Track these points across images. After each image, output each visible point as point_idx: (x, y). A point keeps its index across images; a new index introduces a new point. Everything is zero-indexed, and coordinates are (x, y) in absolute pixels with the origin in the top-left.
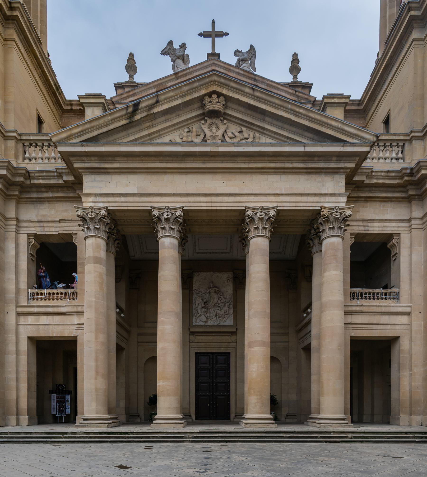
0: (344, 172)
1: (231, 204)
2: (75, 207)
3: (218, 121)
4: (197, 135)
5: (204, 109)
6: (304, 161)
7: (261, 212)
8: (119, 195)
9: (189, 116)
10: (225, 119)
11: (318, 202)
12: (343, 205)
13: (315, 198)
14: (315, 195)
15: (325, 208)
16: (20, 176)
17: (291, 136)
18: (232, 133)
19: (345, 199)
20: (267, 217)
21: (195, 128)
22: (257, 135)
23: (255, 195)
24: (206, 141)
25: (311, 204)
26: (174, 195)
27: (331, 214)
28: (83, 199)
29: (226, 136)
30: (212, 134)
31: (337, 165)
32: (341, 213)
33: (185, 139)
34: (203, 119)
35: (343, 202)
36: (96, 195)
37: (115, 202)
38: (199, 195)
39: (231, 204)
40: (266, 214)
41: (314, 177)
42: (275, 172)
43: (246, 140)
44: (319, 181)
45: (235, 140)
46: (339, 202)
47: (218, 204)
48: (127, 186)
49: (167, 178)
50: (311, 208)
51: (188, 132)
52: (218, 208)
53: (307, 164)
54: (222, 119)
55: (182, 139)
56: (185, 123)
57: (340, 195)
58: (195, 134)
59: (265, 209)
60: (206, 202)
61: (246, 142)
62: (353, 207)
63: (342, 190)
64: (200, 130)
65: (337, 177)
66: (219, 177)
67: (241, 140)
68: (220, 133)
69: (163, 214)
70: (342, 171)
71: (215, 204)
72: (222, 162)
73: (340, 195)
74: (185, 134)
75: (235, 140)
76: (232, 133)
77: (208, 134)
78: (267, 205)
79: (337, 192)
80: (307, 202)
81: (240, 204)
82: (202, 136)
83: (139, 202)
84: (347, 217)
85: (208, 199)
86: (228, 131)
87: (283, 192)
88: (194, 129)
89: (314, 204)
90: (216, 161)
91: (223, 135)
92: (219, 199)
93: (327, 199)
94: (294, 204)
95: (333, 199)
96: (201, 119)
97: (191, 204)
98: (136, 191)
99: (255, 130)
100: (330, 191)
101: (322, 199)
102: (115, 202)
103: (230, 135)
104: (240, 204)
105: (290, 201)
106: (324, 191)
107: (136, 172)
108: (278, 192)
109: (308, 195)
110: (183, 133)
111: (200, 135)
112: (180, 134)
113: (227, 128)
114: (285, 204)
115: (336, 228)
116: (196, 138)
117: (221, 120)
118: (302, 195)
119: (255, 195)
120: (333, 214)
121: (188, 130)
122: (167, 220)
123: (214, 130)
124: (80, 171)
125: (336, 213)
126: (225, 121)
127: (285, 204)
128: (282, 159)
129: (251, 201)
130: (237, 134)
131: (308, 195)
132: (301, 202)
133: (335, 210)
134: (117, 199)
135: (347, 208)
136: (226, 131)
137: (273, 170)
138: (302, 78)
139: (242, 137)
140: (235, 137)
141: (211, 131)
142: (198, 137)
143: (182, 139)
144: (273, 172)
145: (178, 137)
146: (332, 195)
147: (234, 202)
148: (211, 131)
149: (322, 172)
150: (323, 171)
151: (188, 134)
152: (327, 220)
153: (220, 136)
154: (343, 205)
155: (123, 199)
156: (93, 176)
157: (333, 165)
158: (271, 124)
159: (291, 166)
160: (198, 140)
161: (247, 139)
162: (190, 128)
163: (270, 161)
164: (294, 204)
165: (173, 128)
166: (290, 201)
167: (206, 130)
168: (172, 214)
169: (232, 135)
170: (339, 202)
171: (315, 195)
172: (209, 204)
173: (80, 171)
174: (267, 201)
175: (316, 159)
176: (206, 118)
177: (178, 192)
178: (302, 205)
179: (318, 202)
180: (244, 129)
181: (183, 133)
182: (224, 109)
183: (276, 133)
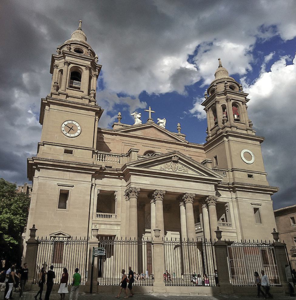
1: (180, 191)
11: (207, 193)
19: (215, 193)
39: (180, 191)
47: (176, 190)
68: (176, 167)
77: (173, 166)
79: (212, 191)
92: (177, 188)
93: (210, 192)
95: (211, 192)
98: (149, 183)
101: (208, 192)
153: (176, 168)
155: (145, 185)
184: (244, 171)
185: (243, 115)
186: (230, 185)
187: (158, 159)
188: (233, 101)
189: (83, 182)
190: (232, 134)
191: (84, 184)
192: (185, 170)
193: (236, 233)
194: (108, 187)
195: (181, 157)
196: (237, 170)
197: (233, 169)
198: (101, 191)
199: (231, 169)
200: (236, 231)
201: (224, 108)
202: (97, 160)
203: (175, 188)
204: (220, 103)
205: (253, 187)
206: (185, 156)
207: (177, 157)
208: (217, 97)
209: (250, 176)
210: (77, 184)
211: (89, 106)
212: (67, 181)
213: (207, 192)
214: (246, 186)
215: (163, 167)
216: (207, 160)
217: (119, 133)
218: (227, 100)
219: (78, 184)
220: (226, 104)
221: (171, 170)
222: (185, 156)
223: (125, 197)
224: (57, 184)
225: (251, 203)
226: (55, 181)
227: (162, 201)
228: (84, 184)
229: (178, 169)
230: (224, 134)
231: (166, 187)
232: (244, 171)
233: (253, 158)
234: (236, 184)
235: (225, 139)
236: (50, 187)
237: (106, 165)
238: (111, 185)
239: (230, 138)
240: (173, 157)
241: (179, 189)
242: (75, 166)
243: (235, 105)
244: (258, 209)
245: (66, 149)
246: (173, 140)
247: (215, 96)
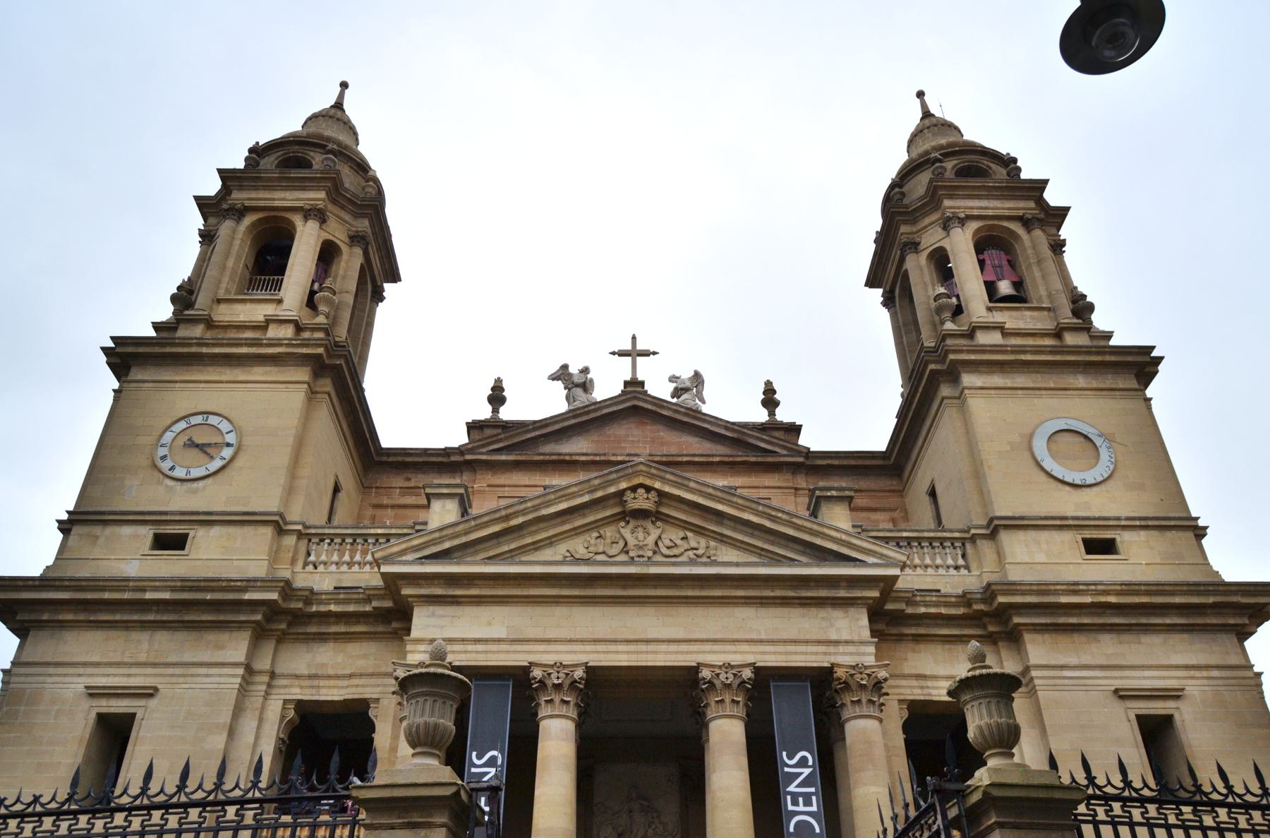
0: (865, 604)
2: (393, 663)
3: (649, 525)
4: (613, 543)
5: (624, 506)
7: (726, 673)
9: (599, 516)
10: (658, 519)
11: (825, 654)
12: (870, 660)
13: (820, 647)
14: (819, 642)
15: (839, 665)
17: (766, 546)
18: (671, 540)
19: (872, 649)
20: (737, 682)
21: (609, 532)
22: (712, 544)
23: (715, 641)
24: (627, 552)
25: (813, 658)
26: (571, 641)
27: (852, 675)
28: (409, 647)
29: (660, 544)
30: (638, 543)
31: (849, 593)
32: (869, 675)
33: (591, 549)
34: (623, 519)
35: (869, 654)
37: (466, 652)
38: (616, 641)
40: (735, 675)
41: (814, 611)
42: (746, 603)
43: (695, 551)
44: (823, 618)
45: (675, 551)
46: (864, 654)
47: (650, 657)
48: (489, 624)
49: (560, 611)
50: (815, 665)
51: (597, 538)
52: (649, 664)
53: (799, 591)
54: (654, 519)
55: (587, 548)
56: (594, 526)
57: (862, 643)
58: (608, 541)
59: (732, 667)
60: (628, 652)
61: (695, 555)
62: (888, 664)
63: (866, 633)
64: (618, 536)
65: (852, 611)
66: (650, 610)
67: (685, 551)
68: (651, 540)
69: (549, 674)
70: (859, 602)
71: (644, 657)
72: (655, 587)
73: (862, 643)
74: (593, 542)
75: (675, 551)
76: (671, 540)
77: (632, 542)
78: (736, 659)
79: (856, 638)
80: (806, 653)
81: (689, 657)
82: (621, 544)
83: (508, 652)
84: (879, 682)
85: (632, 647)
86: (663, 536)
87: (763, 637)
88: (608, 534)
89: (819, 658)
90: (646, 586)
91: (656, 543)
92: (651, 647)
93: (841, 649)
94: (783, 658)
95: (851, 649)
96: (620, 520)
97: (602, 657)
98: (503, 636)
99: (708, 536)
100: (845, 636)
101: (832, 649)
102: (466, 652)
103: (668, 543)
104: (689, 657)
105: (775, 653)
106: (834, 637)
107: (508, 602)
108: (754, 636)
109: (807, 642)
110: (589, 539)
111: (617, 543)
112: (585, 540)
113: (662, 533)
114: (768, 657)
115: (864, 701)
116: (612, 547)
117: (652, 522)
118: (795, 642)
119: (715, 641)
120: (856, 676)
121: (597, 535)
122: (558, 687)
123: (641, 535)
124: (410, 599)
125: (859, 675)
126: (659, 524)
127: (768, 657)
128: (757, 583)
129: (709, 652)
130: (679, 542)
131: (807, 642)
132: (796, 653)
133: (857, 669)
134: (470, 647)
135: (878, 666)
136: (660, 537)
137: (743, 601)
138: (783, 415)
139: (687, 546)
140: (676, 545)
141: (637, 538)
142: (615, 545)
143: (587, 548)
144: (743, 603)
145: (581, 546)
146: (847, 642)
147: (677, 652)
148: (637, 538)
149: (826, 604)
150: (826, 601)
151: (599, 540)
152: (847, 686)
154: (870, 660)
155: (480, 647)
156: (431, 608)
157: (842, 593)
158: (734, 529)
159: (772, 594)
160: (615, 550)
161: (697, 549)
162: (602, 532)
163: (737, 587)
164: (783, 658)
165: (573, 533)
166: (775, 653)
167: (628, 535)
168: (567, 674)
169: (670, 544)
170: (864, 654)
171: (819, 642)
172: (634, 657)
173: (410, 599)
174: (735, 652)
175: (812, 584)
176: (627, 519)
177: (578, 636)
178: (798, 659)
179: (825, 654)
180: (689, 534)
181: (589, 539)
182: (657, 507)
183: (742, 542)
184: (1059, 524)
185: (1037, 274)
186: (976, 607)
187: (545, 512)
188: (974, 225)
189: (203, 671)
190: (973, 357)
191: (207, 676)
192: (700, 552)
194: (332, 682)
195: (667, 489)
196: (1019, 524)
197: (991, 520)
199: (987, 527)
202: (306, 564)
203: (643, 647)
204: (922, 247)
205: (1112, 599)
206: (686, 482)
208: (904, 229)
209: (1100, 547)
210: (174, 680)
211: (281, 345)
212: (134, 671)
213: (822, 649)
214: (1064, 599)
215: (581, 552)
216: (821, 489)
217: (484, 457)
219: (181, 680)
221: (623, 558)
222: (679, 480)
224: (87, 687)
225: (1116, 691)
226: (80, 675)
227: (573, 719)
228: (207, 676)
229: (665, 551)
230: (932, 366)
231: (589, 648)
232: (1059, 524)
233: (1104, 454)
236: (56, 708)
237: (340, 580)
238: (348, 672)
239: (968, 379)
240: (629, 496)
241: (663, 647)
242: (166, 596)
244: (1168, 720)
245: (161, 531)
246: (734, 453)
247: (897, 229)
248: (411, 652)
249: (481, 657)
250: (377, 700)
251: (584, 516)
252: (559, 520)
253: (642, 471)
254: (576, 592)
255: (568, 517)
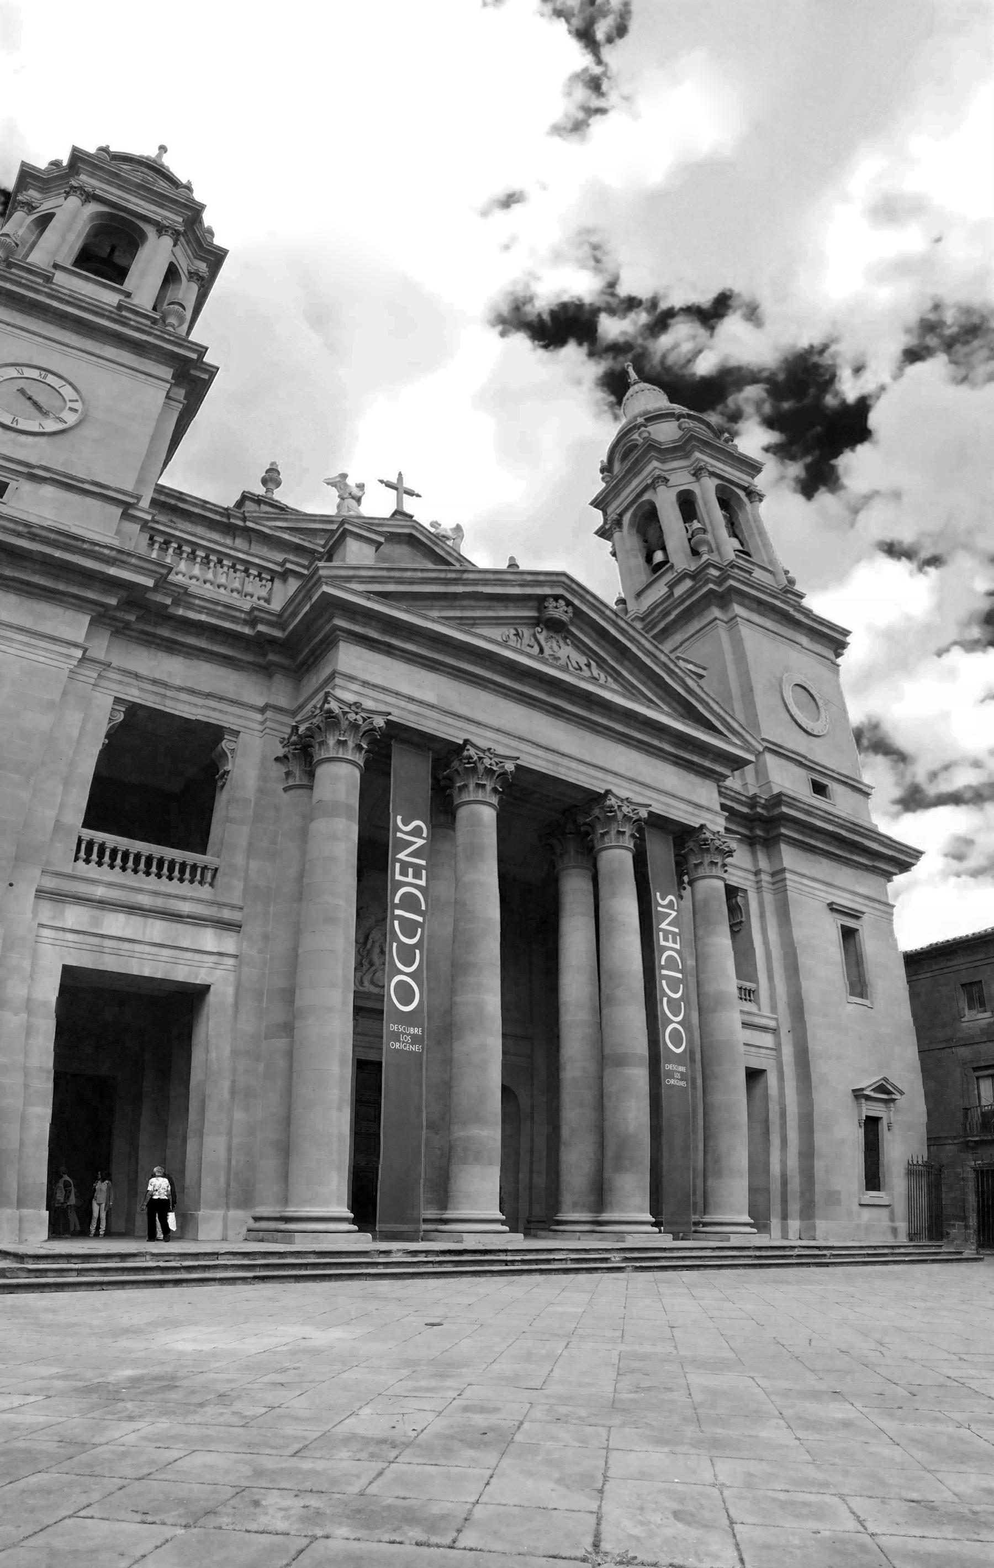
6: (677, 746)
8: (409, 698)
16: (166, 594)
18: (577, 663)
36: (365, 683)
76: (577, 663)
77: (547, 651)
130: (584, 668)
157: (707, 764)
159: (660, 745)
162: (519, 630)
167: (543, 643)
175: (690, 747)
180: (593, 663)
193: (775, 1031)
198: (133, 710)
200: (772, 1024)
201: (687, 506)
207: (569, 603)
213: (690, 809)
218: (697, 473)
220: (695, 488)
223: (281, 769)
234: (790, 806)
235: (716, 612)
243: (727, 501)
248: (343, 688)
249: (412, 718)
250: (237, 733)
251: (507, 608)
252: (486, 604)
253: (563, 583)
254: (507, 682)
255: (494, 604)
